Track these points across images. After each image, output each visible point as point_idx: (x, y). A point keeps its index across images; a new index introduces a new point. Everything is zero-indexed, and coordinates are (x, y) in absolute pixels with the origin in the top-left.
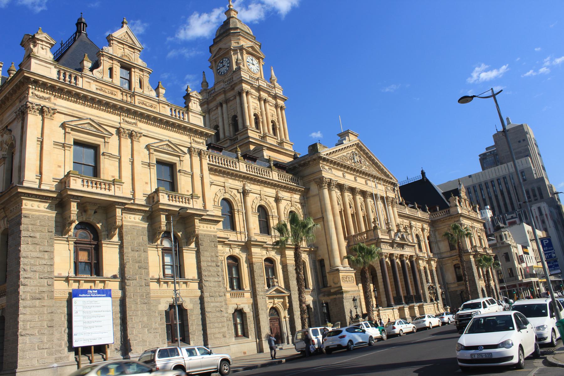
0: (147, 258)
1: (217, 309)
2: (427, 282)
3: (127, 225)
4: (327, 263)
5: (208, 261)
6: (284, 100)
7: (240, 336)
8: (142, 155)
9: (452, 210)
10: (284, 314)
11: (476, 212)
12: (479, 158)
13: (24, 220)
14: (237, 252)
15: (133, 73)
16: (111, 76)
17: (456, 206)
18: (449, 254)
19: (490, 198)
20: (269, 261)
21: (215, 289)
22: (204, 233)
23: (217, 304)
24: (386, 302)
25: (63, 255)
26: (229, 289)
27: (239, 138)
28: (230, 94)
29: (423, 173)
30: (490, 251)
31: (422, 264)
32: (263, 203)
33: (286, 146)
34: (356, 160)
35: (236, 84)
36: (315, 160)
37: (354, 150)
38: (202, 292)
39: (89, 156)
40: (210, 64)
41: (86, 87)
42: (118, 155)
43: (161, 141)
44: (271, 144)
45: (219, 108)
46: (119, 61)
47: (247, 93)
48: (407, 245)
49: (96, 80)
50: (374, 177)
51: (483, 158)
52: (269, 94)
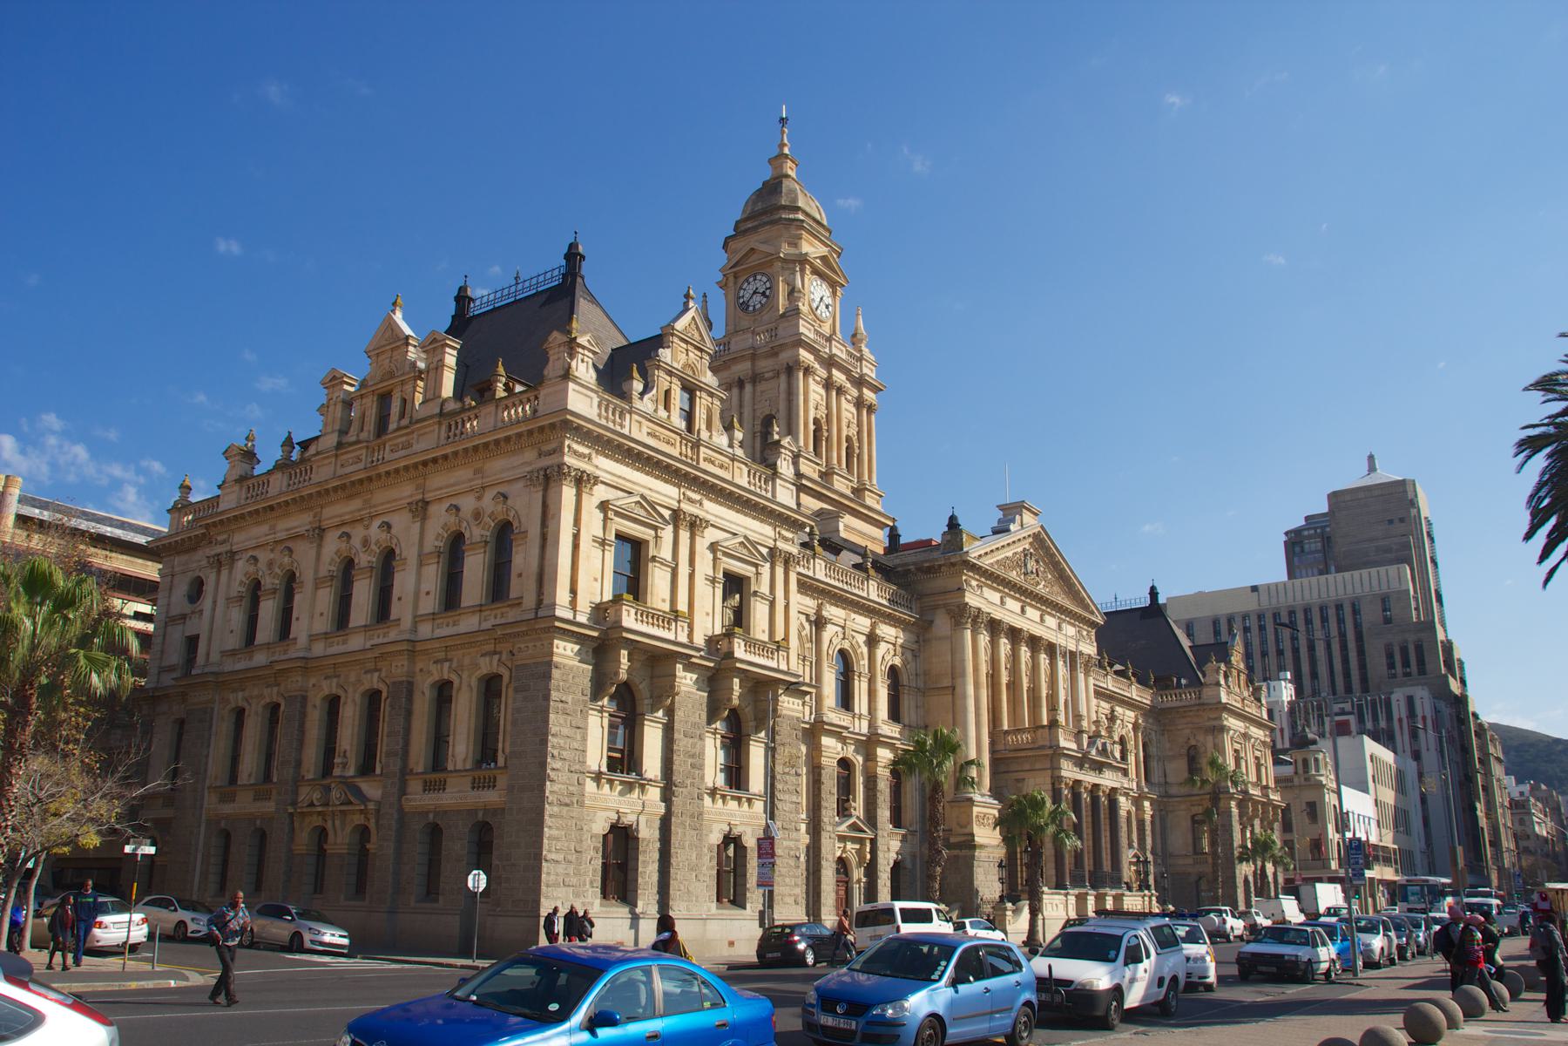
2: (1130, 846)
6: (876, 390)
9: (1207, 693)
10: (858, 874)
11: (1259, 700)
12: (1284, 538)
13: (556, 673)
16: (667, 407)
17: (1218, 684)
18: (1184, 790)
19: (1296, 651)
20: (844, 763)
23: (791, 844)
25: (597, 735)
28: (765, 365)
29: (1153, 593)
30: (1275, 797)
31: (1124, 804)
32: (846, 645)
33: (870, 500)
35: (783, 347)
36: (953, 565)
39: (634, 561)
40: (720, 277)
42: (669, 558)
46: (681, 379)
47: (808, 371)
48: (1110, 766)
51: (1294, 542)
52: (847, 372)
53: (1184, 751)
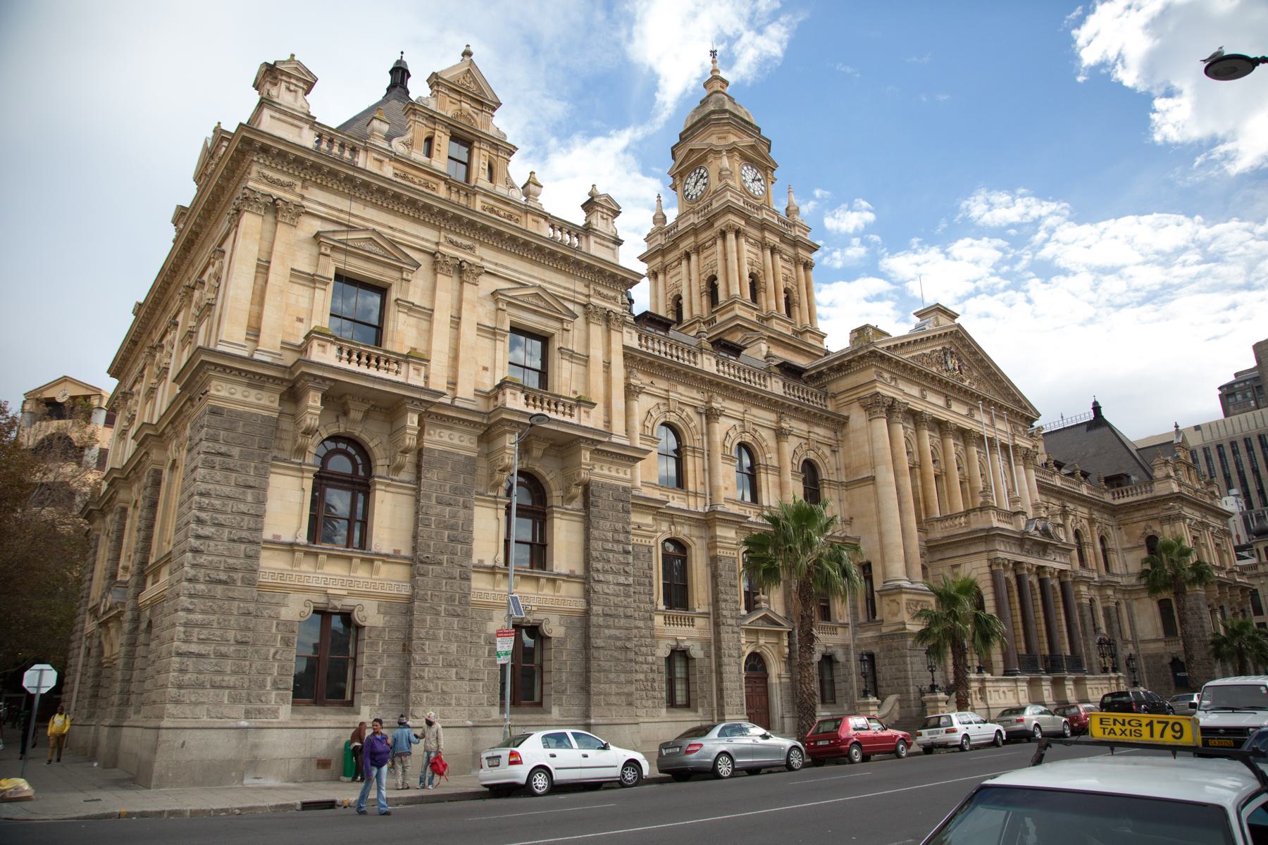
0: (470, 521)
1: (619, 643)
3: (431, 450)
4: (877, 571)
5: (607, 540)
7: (681, 707)
8: (478, 311)
14: (683, 532)
15: (476, 151)
21: (617, 600)
22: (603, 480)
24: (1001, 665)
26: (662, 607)
27: (719, 319)
28: (705, 236)
29: (1096, 408)
34: (951, 366)
37: (947, 346)
38: (588, 603)
40: (671, 181)
41: (372, 166)
43: (524, 286)
44: (781, 334)
45: (684, 263)
49: (395, 158)
50: (988, 402)
53: (1143, 542)
